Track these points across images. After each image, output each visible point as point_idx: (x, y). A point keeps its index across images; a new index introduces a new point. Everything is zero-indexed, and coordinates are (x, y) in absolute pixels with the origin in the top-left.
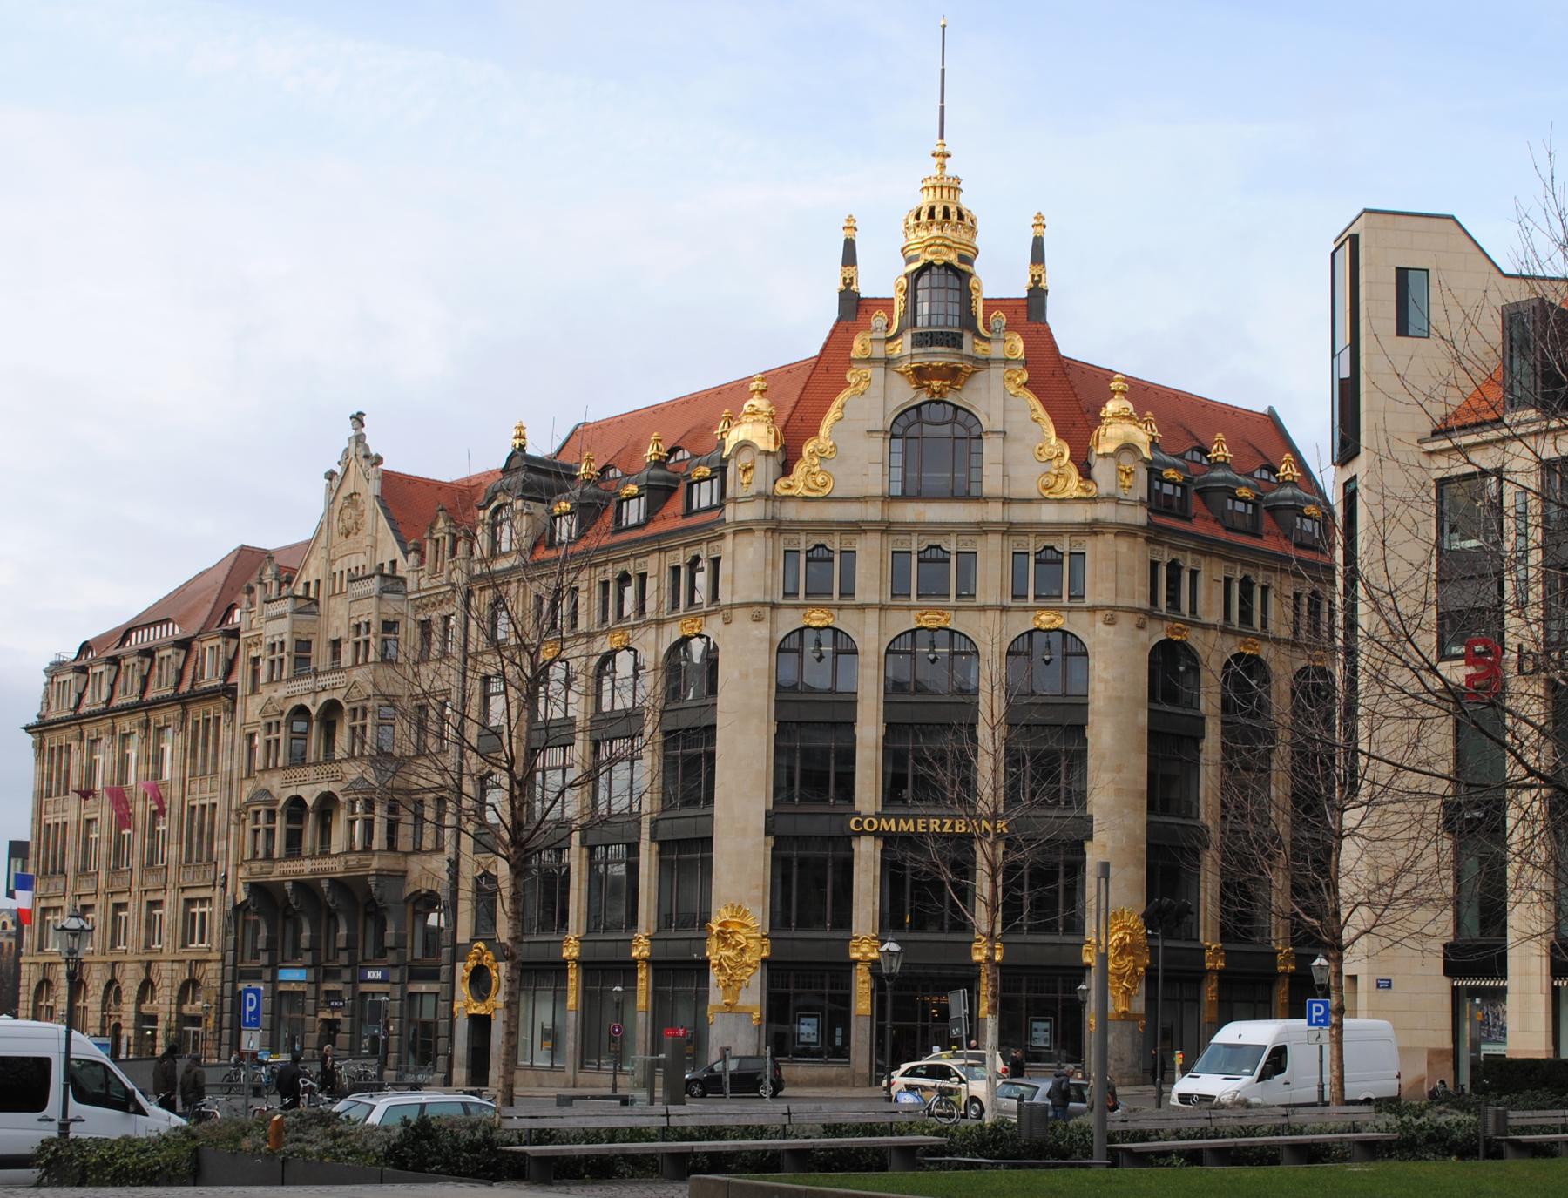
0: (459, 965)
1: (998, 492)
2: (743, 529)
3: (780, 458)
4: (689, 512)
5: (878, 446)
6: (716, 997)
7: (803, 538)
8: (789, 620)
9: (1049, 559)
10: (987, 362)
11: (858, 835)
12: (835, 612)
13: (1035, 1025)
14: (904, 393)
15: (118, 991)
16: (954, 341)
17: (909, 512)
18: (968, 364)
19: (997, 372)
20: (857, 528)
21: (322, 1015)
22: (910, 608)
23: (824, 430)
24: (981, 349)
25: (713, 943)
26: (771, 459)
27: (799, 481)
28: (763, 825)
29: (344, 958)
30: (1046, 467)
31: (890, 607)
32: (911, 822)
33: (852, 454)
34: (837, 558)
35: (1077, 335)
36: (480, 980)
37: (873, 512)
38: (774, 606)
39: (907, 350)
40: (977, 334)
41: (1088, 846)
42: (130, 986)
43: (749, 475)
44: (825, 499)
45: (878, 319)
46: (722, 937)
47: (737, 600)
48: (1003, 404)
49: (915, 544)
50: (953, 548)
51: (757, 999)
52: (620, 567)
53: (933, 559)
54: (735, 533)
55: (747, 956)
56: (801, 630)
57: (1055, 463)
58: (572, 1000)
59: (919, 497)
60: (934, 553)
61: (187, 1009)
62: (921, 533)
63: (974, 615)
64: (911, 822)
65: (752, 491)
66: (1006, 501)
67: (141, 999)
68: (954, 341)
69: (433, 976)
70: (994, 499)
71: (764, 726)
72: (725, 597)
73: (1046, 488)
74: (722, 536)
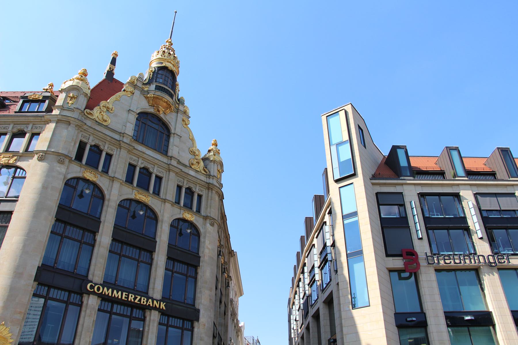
5: (133, 118)
8: (76, 170)
9: (190, 192)
11: (89, 293)
27: (96, 113)
28: (34, 274)
32: (120, 293)
41: (196, 324)
44: (106, 127)
53: (146, 173)
64: (120, 293)
71: (50, 218)
73: (192, 164)
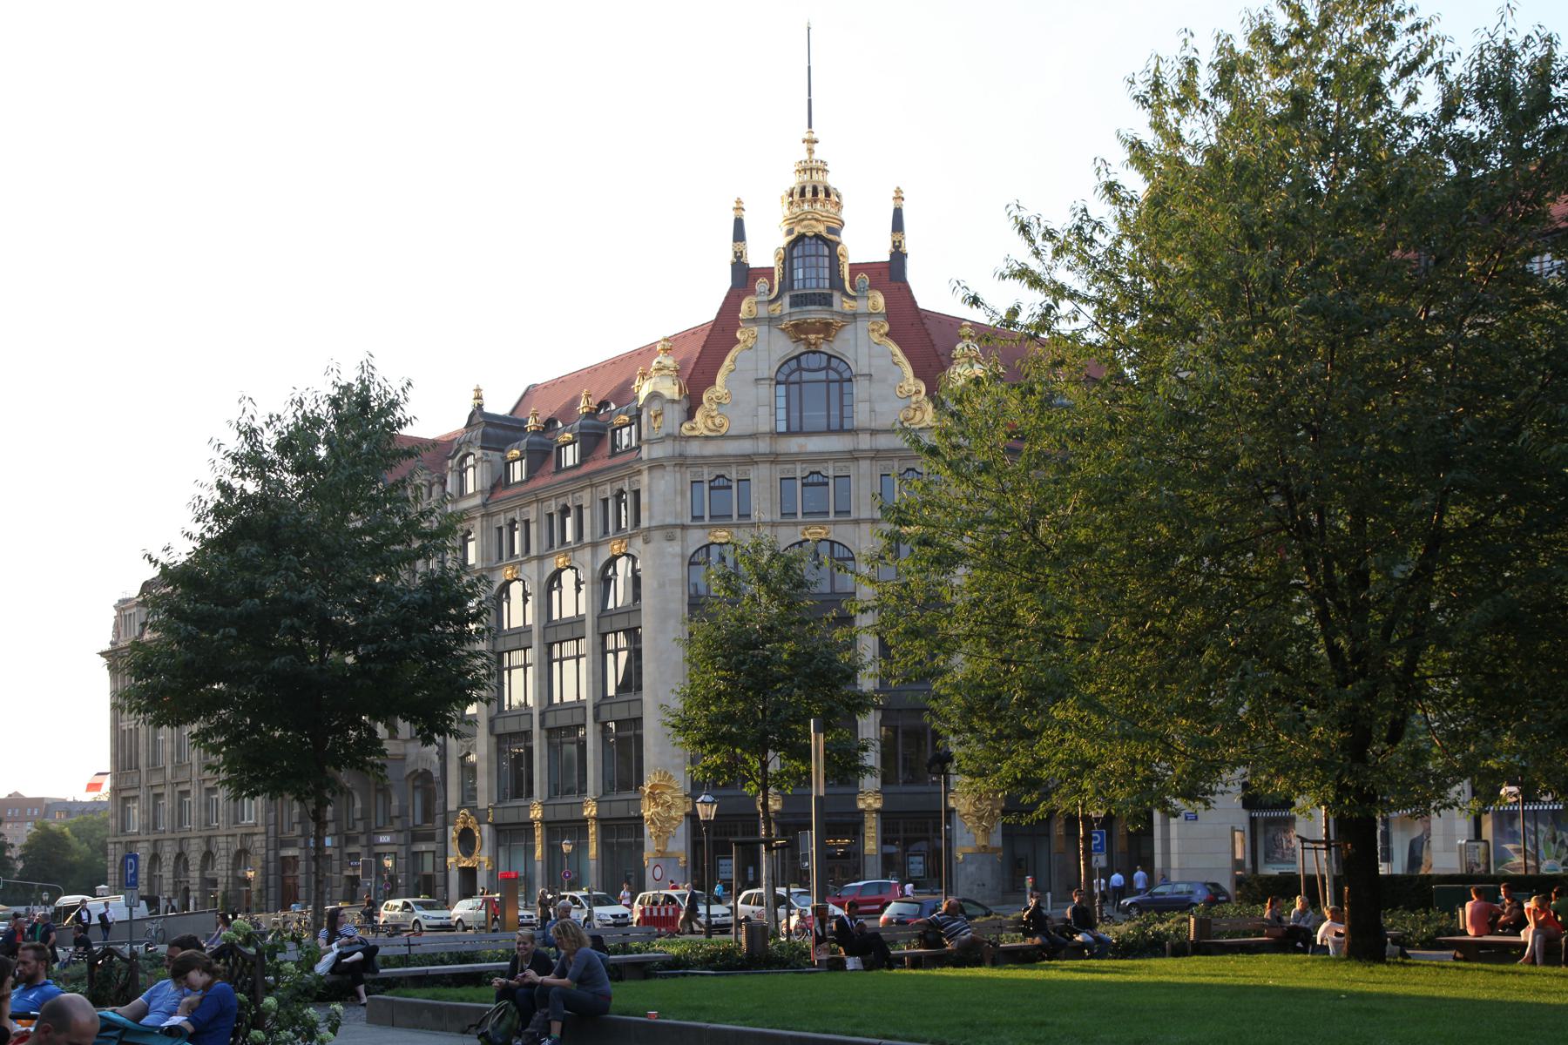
0: (450, 828)
1: (867, 425)
2: (656, 465)
3: (685, 405)
4: (614, 454)
6: (650, 846)
7: (706, 470)
8: (697, 538)
10: (855, 316)
12: (734, 530)
13: (911, 859)
14: (784, 347)
15: (186, 861)
16: (825, 300)
17: (794, 445)
18: (838, 319)
19: (863, 325)
20: (749, 460)
21: (347, 873)
22: (796, 524)
23: (720, 379)
24: (848, 306)
25: (646, 802)
26: (676, 407)
29: (360, 827)
30: (906, 402)
31: (780, 524)
33: (743, 399)
34: (734, 486)
35: (932, 291)
36: (467, 840)
37: (763, 446)
38: (684, 527)
39: (787, 309)
40: (845, 294)
42: (195, 858)
43: (660, 419)
44: (724, 437)
45: (761, 285)
46: (652, 796)
47: (654, 524)
48: (869, 349)
49: (799, 471)
50: (831, 473)
51: (682, 846)
52: (562, 501)
53: (814, 482)
54: (650, 468)
55: (673, 813)
56: (707, 546)
57: (914, 399)
58: (538, 852)
59: (801, 432)
60: (815, 478)
61: (240, 873)
62: (803, 461)
63: (850, 528)
65: (662, 433)
66: (874, 432)
67: (203, 868)
68: (825, 300)
69: (430, 837)
70: (864, 430)
72: (644, 523)
74: (639, 472)
